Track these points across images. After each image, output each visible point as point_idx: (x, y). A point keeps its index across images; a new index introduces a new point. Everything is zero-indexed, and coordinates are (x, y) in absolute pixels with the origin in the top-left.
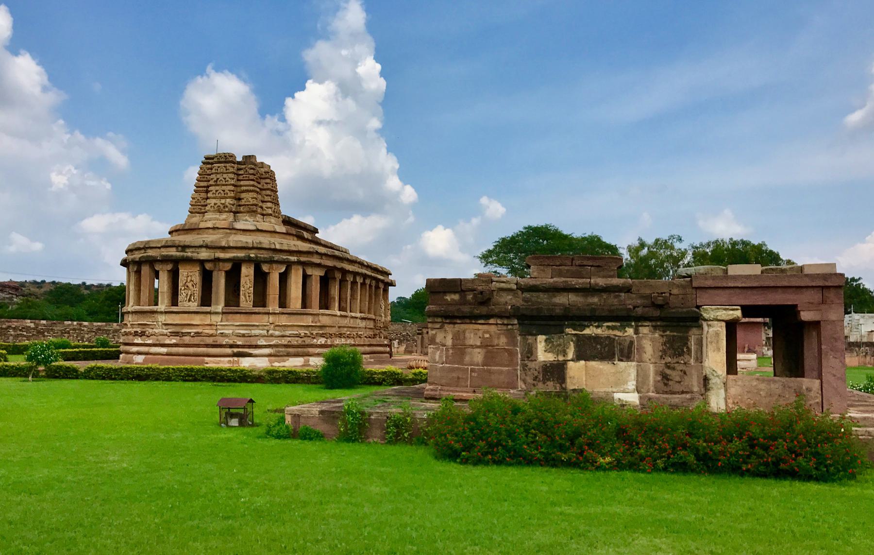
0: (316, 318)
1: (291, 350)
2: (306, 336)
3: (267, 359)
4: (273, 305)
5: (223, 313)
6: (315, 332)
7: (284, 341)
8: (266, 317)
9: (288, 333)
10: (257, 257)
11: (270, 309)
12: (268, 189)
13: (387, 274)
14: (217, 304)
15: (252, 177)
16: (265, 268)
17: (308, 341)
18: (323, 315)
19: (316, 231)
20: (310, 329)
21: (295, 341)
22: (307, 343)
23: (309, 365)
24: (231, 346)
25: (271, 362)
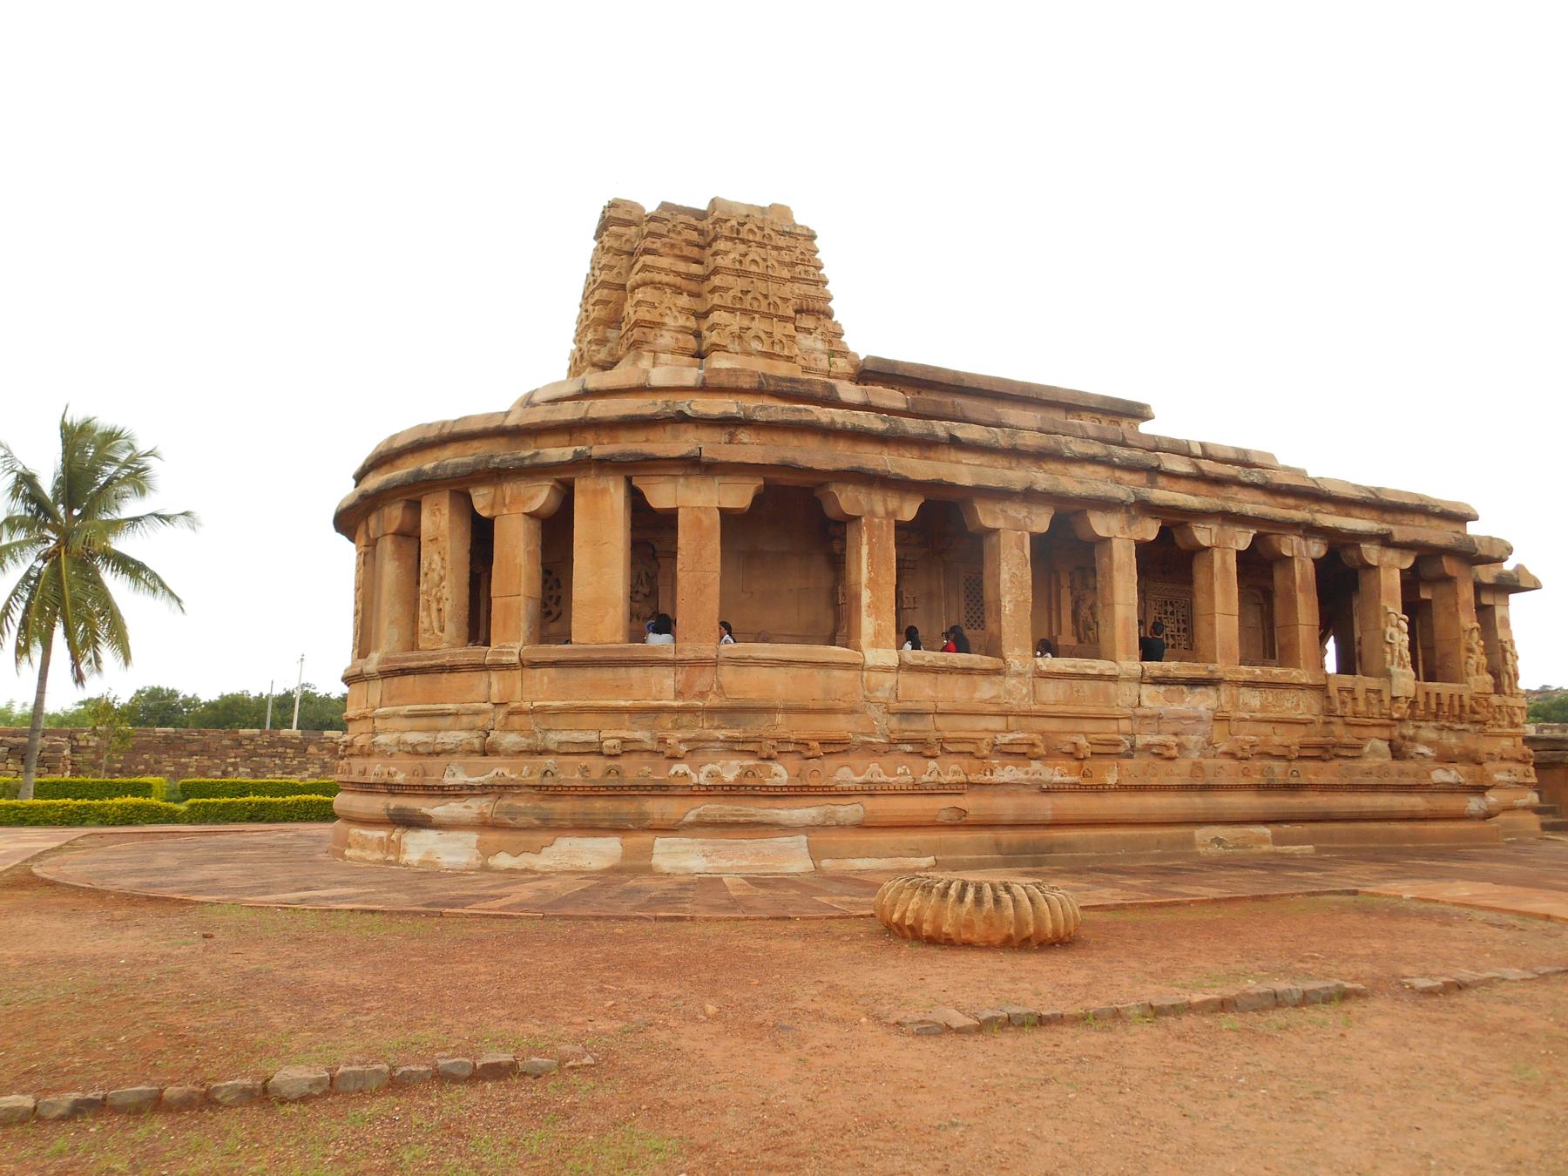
0: (704, 679)
1: (561, 807)
2: (628, 748)
3: (473, 837)
4: (512, 634)
5: (386, 674)
6: (673, 737)
7: (526, 771)
8: (479, 679)
9: (554, 738)
10: (435, 468)
11: (489, 654)
12: (716, 271)
13: (1459, 517)
14: (377, 648)
15: (657, 244)
16: (482, 500)
17: (636, 770)
18: (740, 662)
19: (1138, 412)
20: (667, 721)
21: (570, 772)
22: (631, 777)
23: (649, 870)
24: (392, 789)
25: (486, 851)
